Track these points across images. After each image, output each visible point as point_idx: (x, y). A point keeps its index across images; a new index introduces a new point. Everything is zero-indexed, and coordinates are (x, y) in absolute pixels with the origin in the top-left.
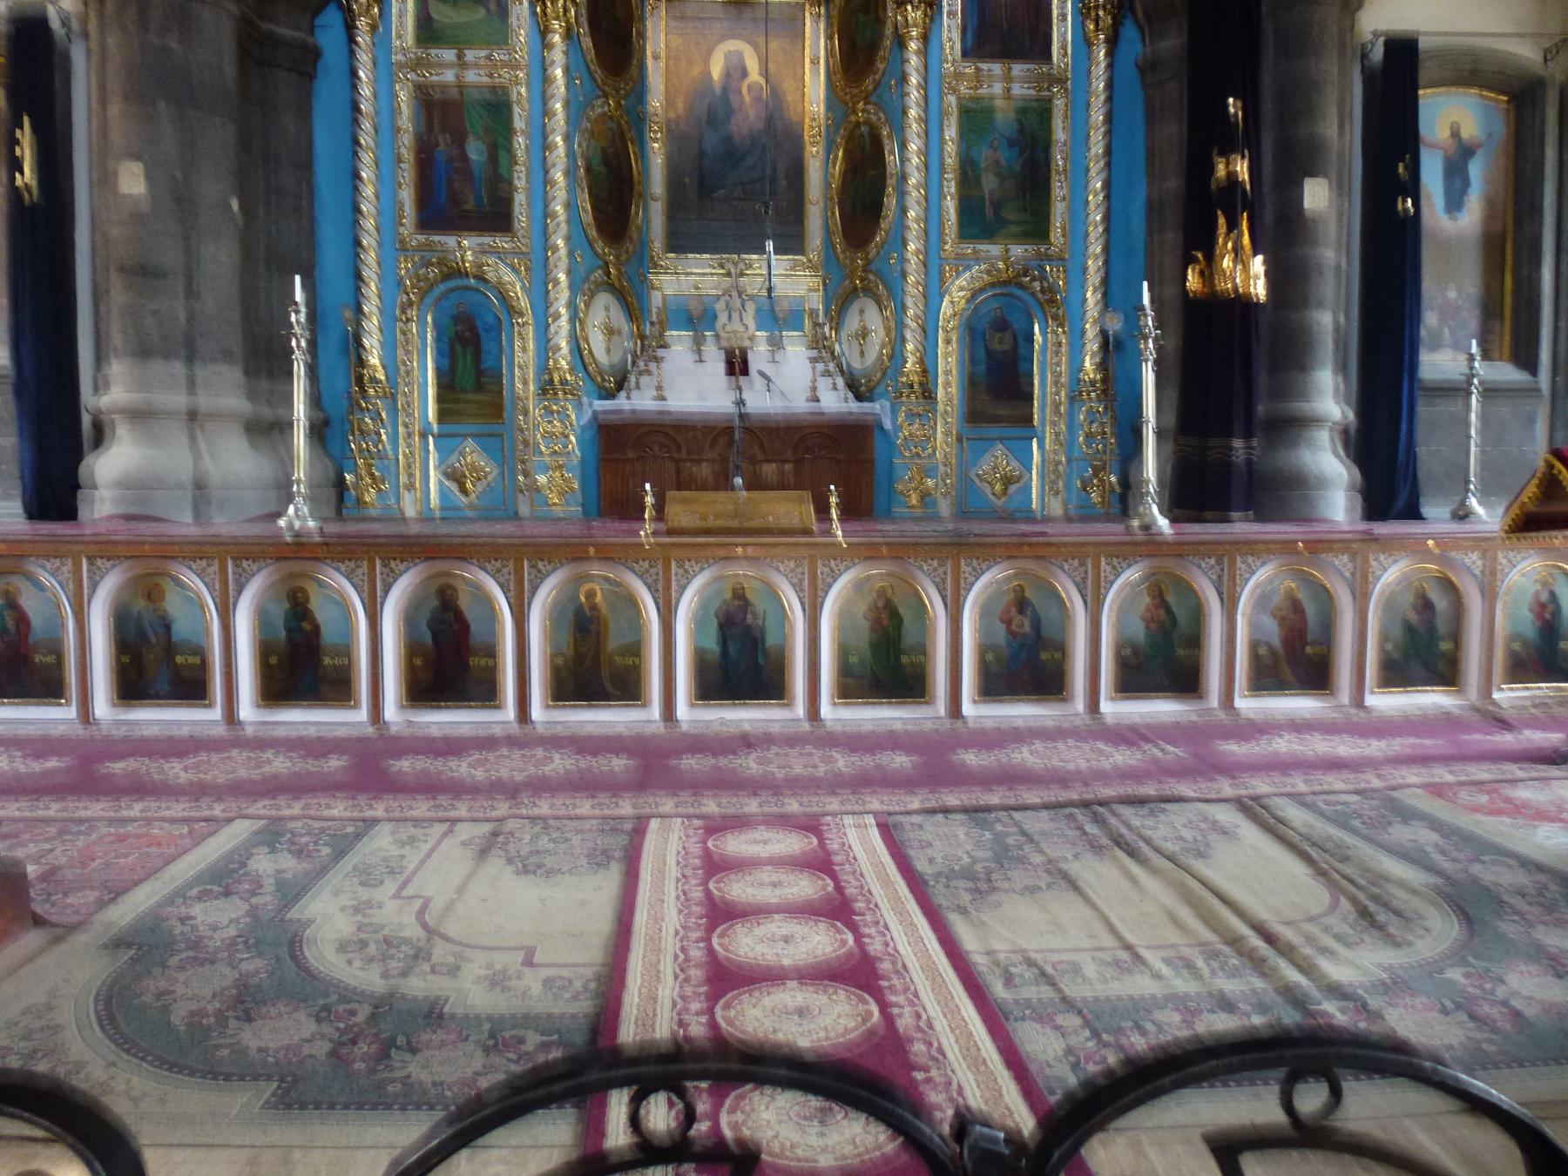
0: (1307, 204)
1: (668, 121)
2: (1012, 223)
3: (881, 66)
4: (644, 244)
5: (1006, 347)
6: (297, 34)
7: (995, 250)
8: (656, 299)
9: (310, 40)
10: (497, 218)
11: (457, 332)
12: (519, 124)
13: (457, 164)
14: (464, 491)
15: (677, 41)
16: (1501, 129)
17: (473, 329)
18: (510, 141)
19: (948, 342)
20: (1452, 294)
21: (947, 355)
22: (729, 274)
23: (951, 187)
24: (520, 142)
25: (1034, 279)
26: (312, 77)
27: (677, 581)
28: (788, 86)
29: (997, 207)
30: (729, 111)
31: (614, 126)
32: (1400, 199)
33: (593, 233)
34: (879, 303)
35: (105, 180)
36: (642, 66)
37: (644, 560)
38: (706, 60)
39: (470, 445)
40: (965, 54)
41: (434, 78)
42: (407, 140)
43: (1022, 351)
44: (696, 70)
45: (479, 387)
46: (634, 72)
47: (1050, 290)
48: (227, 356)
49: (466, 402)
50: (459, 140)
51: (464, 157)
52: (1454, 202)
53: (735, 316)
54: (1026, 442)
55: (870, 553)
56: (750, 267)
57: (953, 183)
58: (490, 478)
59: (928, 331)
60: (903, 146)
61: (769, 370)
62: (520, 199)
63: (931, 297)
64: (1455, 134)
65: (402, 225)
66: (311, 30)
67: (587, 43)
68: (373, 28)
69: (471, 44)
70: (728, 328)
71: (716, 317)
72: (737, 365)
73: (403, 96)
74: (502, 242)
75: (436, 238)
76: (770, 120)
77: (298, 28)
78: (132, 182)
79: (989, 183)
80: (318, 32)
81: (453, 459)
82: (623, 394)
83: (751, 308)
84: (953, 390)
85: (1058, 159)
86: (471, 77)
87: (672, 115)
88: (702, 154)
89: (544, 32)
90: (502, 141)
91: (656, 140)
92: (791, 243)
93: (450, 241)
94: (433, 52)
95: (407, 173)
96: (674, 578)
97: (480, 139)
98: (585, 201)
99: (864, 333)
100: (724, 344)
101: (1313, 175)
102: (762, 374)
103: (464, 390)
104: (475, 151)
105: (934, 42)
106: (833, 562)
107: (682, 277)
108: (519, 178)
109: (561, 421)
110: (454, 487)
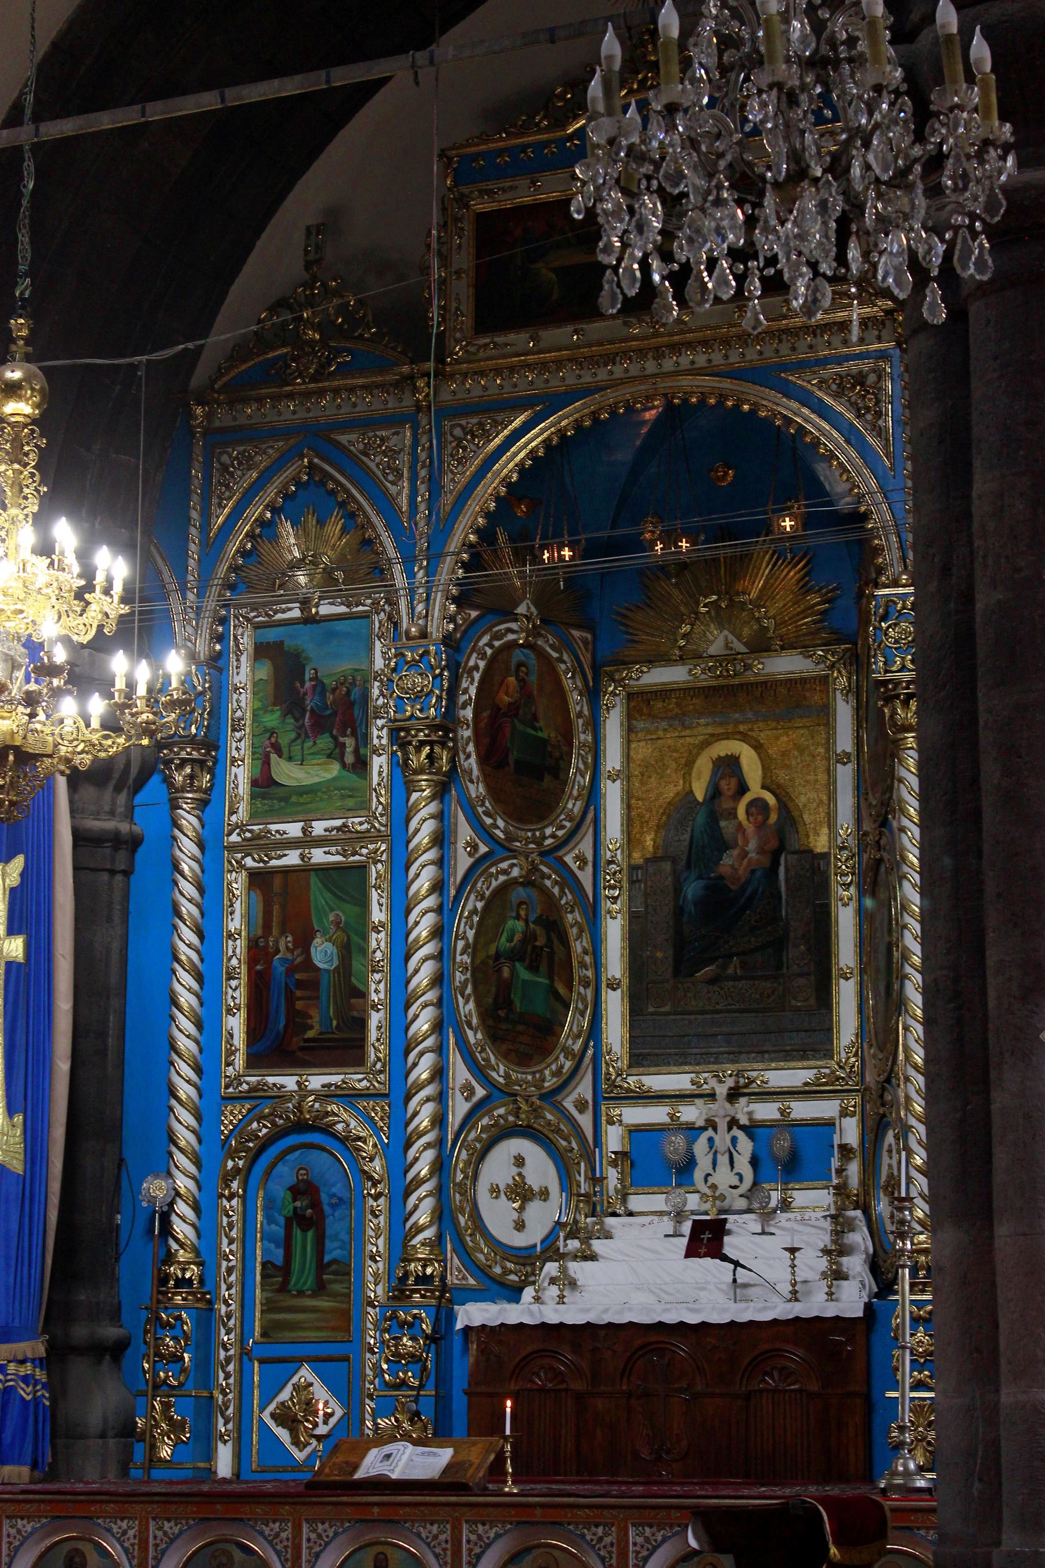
6: (110, 825)
8: (614, 1139)
9: (124, 827)
11: (295, 1209)
12: (378, 915)
13: (297, 976)
14: (296, 1442)
15: (642, 750)
17: (316, 1205)
18: (366, 938)
22: (712, 1096)
24: (378, 942)
26: (127, 873)
27: (310, 1548)
28: (805, 797)
30: (722, 845)
36: (593, 796)
37: (274, 1522)
38: (687, 776)
39: (305, 1374)
41: (274, 863)
42: (237, 951)
44: (670, 792)
45: (320, 1288)
46: (575, 807)
49: (304, 1310)
50: (304, 942)
51: (308, 964)
56: (753, 1081)
62: (375, 1019)
65: (228, 1065)
66: (129, 815)
68: (202, 804)
70: (711, 1180)
74: (358, 1080)
75: (271, 1080)
77: (112, 813)
80: (137, 810)
81: (285, 1395)
82: (528, 1293)
83: (745, 1145)
86: (318, 856)
87: (637, 857)
88: (679, 911)
89: (410, 787)
90: (355, 939)
91: (614, 900)
93: (290, 1083)
94: (273, 827)
95: (237, 993)
96: (304, 1544)
97: (329, 940)
103: (301, 1293)
106: (480, 1526)
108: (377, 991)
109: (413, 1338)
110: (283, 1434)
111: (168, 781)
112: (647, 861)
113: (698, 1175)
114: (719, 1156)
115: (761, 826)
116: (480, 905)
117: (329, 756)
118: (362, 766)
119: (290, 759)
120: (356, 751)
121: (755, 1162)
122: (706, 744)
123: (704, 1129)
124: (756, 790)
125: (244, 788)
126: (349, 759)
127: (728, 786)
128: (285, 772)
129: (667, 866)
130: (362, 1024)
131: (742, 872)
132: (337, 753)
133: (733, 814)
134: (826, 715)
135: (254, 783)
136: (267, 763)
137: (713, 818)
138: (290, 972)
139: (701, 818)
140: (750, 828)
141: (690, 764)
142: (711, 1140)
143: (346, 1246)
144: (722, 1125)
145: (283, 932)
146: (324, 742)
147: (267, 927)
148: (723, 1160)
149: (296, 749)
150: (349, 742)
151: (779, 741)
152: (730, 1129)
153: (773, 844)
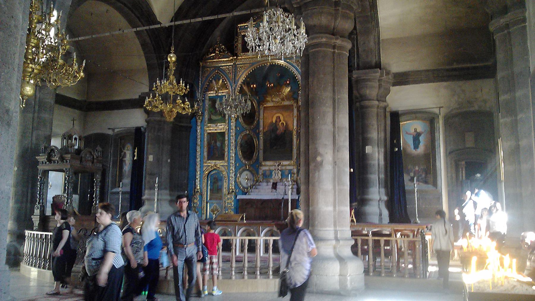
0: (366, 152)
8: (261, 172)
9: (189, 125)
10: (221, 157)
16: (428, 129)
20: (417, 168)
30: (277, 129)
31: (249, 136)
32: (395, 148)
33: (242, 159)
35: (147, 158)
44: (270, 121)
48: (166, 189)
50: (216, 142)
51: (216, 145)
52: (416, 147)
55: (245, 225)
58: (219, 212)
62: (226, 154)
64: (415, 130)
72: (275, 186)
73: (206, 134)
76: (285, 131)
78: (151, 158)
83: (280, 173)
87: (265, 131)
92: (290, 158)
95: (206, 150)
98: (240, 153)
101: (367, 145)
104: (218, 144)
110: (212, 213)
111: (196, 118)
112: (266, 131)
113: (273, 177)
115: (283, 126)
116: (241, 137)
121: (281, 175)
122: (276, 113)
123: (274, 170)
124: (282, 121)
125: (207, 119)
126: (222, 116)
127: (278, 120)
128: (214, 117)
130: (224, 155)
134: (293, 110)
136: (210, 117)
138: (213, 147)
141: (272, 118)
142: (275, 172)
143: (221, 186)
144: (277, 170)
145: (213, 140)
147: (210, 140)
148: (277, 175)
151: (286, 114)
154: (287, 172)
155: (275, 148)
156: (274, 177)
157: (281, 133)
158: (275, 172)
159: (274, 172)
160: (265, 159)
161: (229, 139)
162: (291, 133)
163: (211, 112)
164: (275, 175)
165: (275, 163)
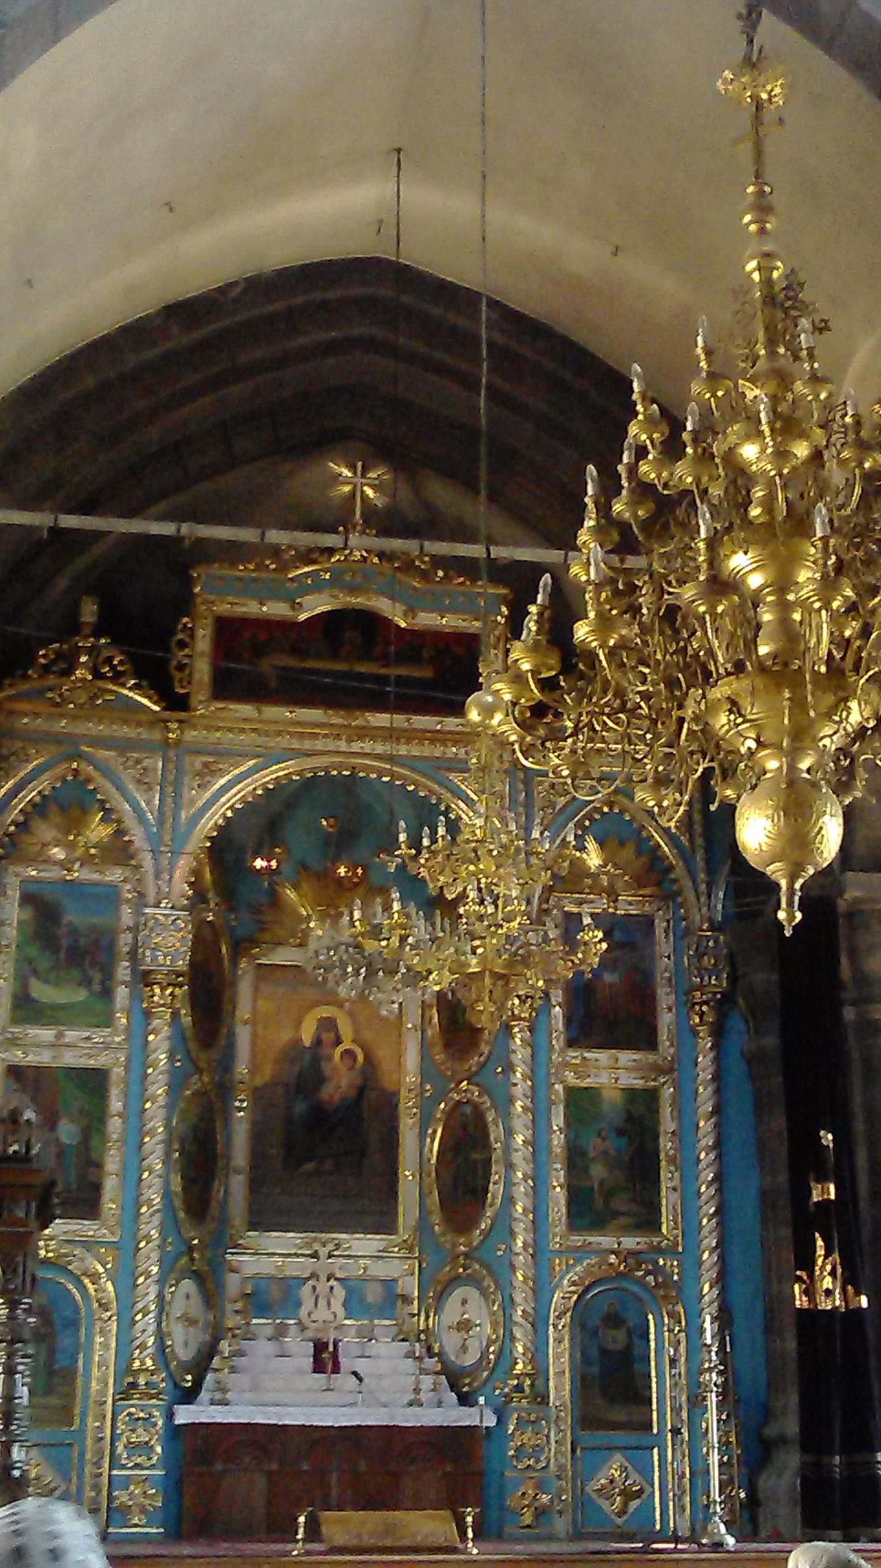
1: (256, 1089)
2: (623, 1214)
3: (485, 1049)
4: (224, 1221)
5: (619, 1346)
7: (606, 1241)
8: (233, 1283)
19: (559, 1341)
21: (558, 1357)
22: (315, 1255)
23: (558, 1177)
25: (648, 1273)
29: (608, 1195)
34: (484, 1292)
36: (231, 1034)
38: (298, 1024)
40: (571, 1043)
43: (636, 1351)
44: (286, 1035)
47: (666, 1284)
53: (322, 1302)
54: (648, 1451)
56: (338, 1246)
57: (562, 1172)
59: (538, 1322)
60: (510, 1133)
61: (361, 1366)
63: (539, 1290)
67: (187, 1021)
69: (71, 1024)
71: (299, 1304)
76: (361, 1091)
79: (598, 1171)
83: (340, 1293)
84: (567, 1393)
85: (666, 1145)
87: (259, 1081)
91: (240, 1109)
99: (465, 1326)
100: (309, 1334)
102: (355, 1374)
105: (541, 1036)
107: (264, 1258)
113: (303, 1312)
114: (320, 1300)
117: (80, 985)
118: (107, 993)
119: (47, 981)
120: (103, 983)
123: (308, 1279)
124: (346, 1045)
126: (97, 987)
128: (41, 991)
129: (280, 1090)
131: (336, 1098)
132: (86, 982)
133: (330, 1058)
135: (15, 996)
137: (316, 1060)
139: (308, 1057)
140: (343, 1068)
142: (314, 1288)
144: (323, 1278)
146: (76, 973)
149: (52, 976)
150: (97, 977)
152: (328, 1280)
153: (359, 1082)
154: (373, 1294)
155: (310, 1166)
156: (309, 1314)
157: (343, 1100)
158: (314, 1288)
159: (306, 1289)
160: (258, 1222)
161: (137, 1118)
162: (389, 1105)
163: (30, 962)
164: (316, 1305)
165: (317, 1246)
